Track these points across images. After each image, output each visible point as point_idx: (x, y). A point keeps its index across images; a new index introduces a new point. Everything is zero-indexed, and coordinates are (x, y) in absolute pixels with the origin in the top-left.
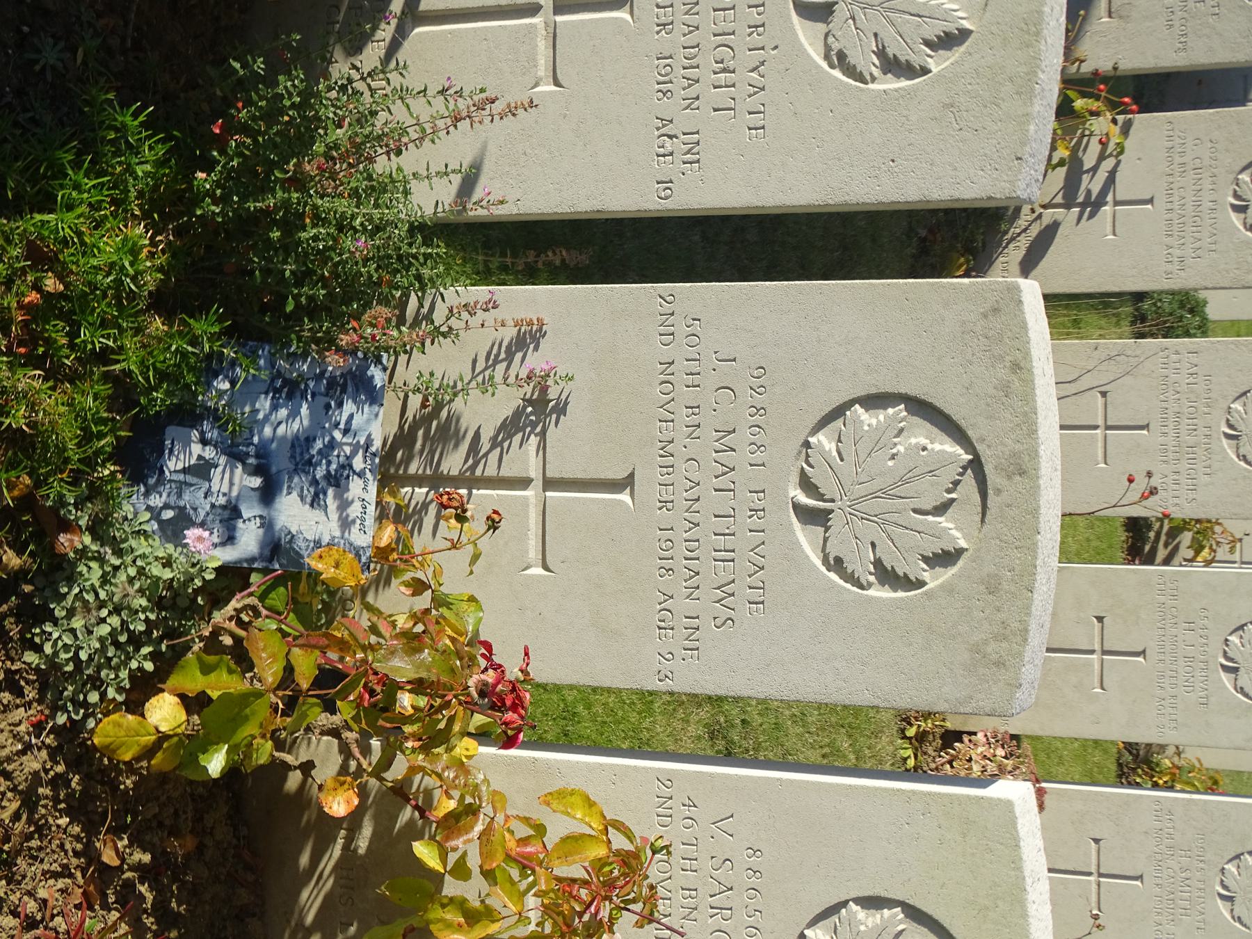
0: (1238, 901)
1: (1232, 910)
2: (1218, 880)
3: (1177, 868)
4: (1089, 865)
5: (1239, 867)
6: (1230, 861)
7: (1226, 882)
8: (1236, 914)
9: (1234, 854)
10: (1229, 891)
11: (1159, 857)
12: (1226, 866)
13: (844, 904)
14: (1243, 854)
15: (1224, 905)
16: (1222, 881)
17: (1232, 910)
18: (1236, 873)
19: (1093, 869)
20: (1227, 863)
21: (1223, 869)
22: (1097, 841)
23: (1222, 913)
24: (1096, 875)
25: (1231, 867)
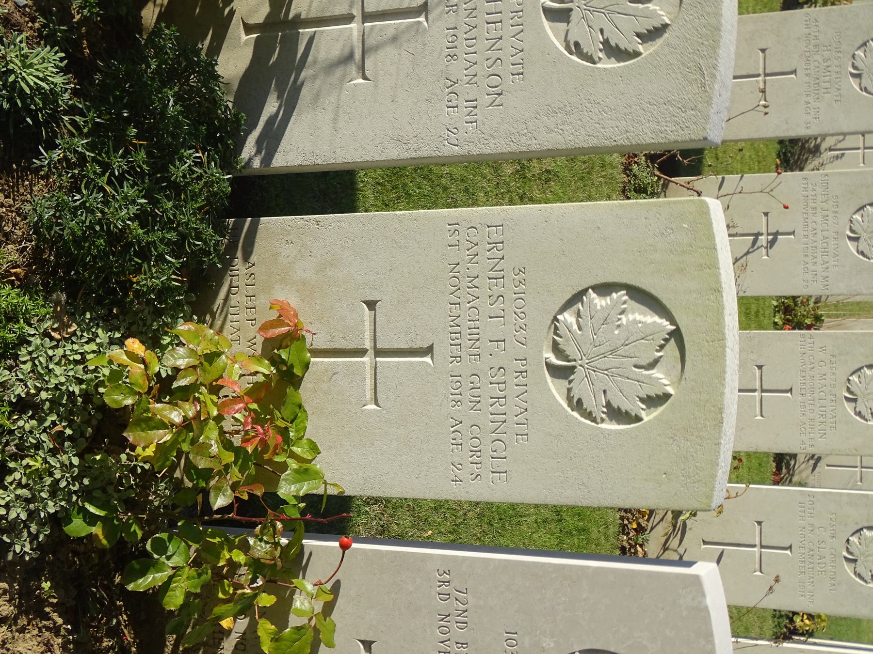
0: (864, 76)
2: (850, 64)
3: (821, 60)
4: (758, 69)
6: (859, 48)
8: (863, 86)
11: (808, 54)
12: (856, 53)
13: (584, 292)
15: (854, 82)
16: (853, 63)
17: (860, 84)
18: (863, 56)
19: (761, 71)
20: (857, 50)
21: (854, 54)
22: (763, 51)
24: (763, 76)
25: (860, 53)
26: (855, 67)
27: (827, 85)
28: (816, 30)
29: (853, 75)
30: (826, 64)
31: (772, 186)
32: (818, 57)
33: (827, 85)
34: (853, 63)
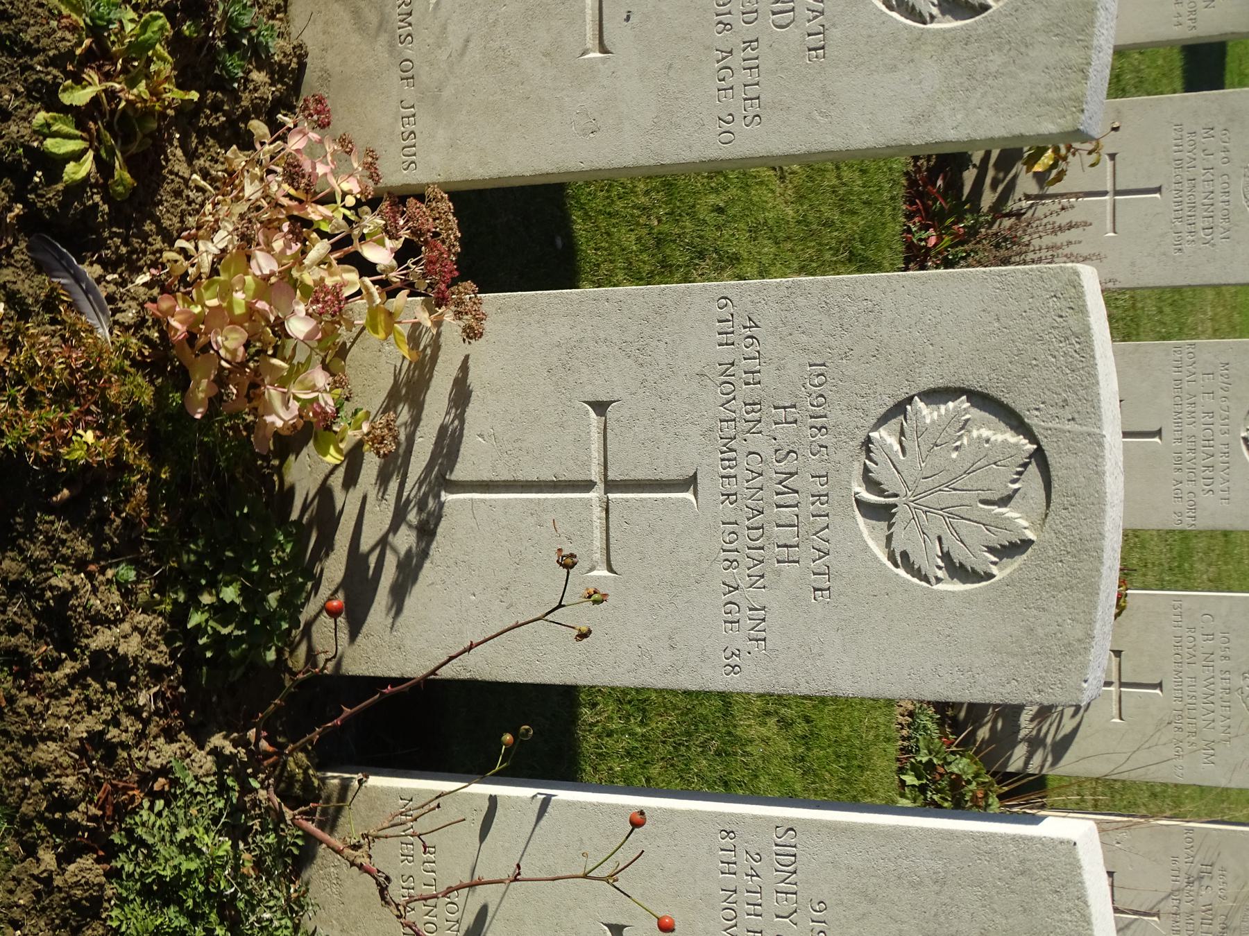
1: (889, 538)
2: (857, 469)
3: (767, 451)
5: (902, 433)
6: (883, 420)
7: (877, 473)
8: (898, 546)
9: (891, 403)
10: (881, 493)
12: (874, 435)
14: (910, 400)
16: (866, 470)
17: (889, 538)
18: (897, 447)
21: (869, 440)
23: (866, 548)
25: (886, 437)
26: (873, 485)
27: (787, 535)
28: (750, 352)
29: (869, 510)
30: (782, 466)
31: (623, 857)
32: (758, 442)
33: (787, 535)
34: (866, 470)
